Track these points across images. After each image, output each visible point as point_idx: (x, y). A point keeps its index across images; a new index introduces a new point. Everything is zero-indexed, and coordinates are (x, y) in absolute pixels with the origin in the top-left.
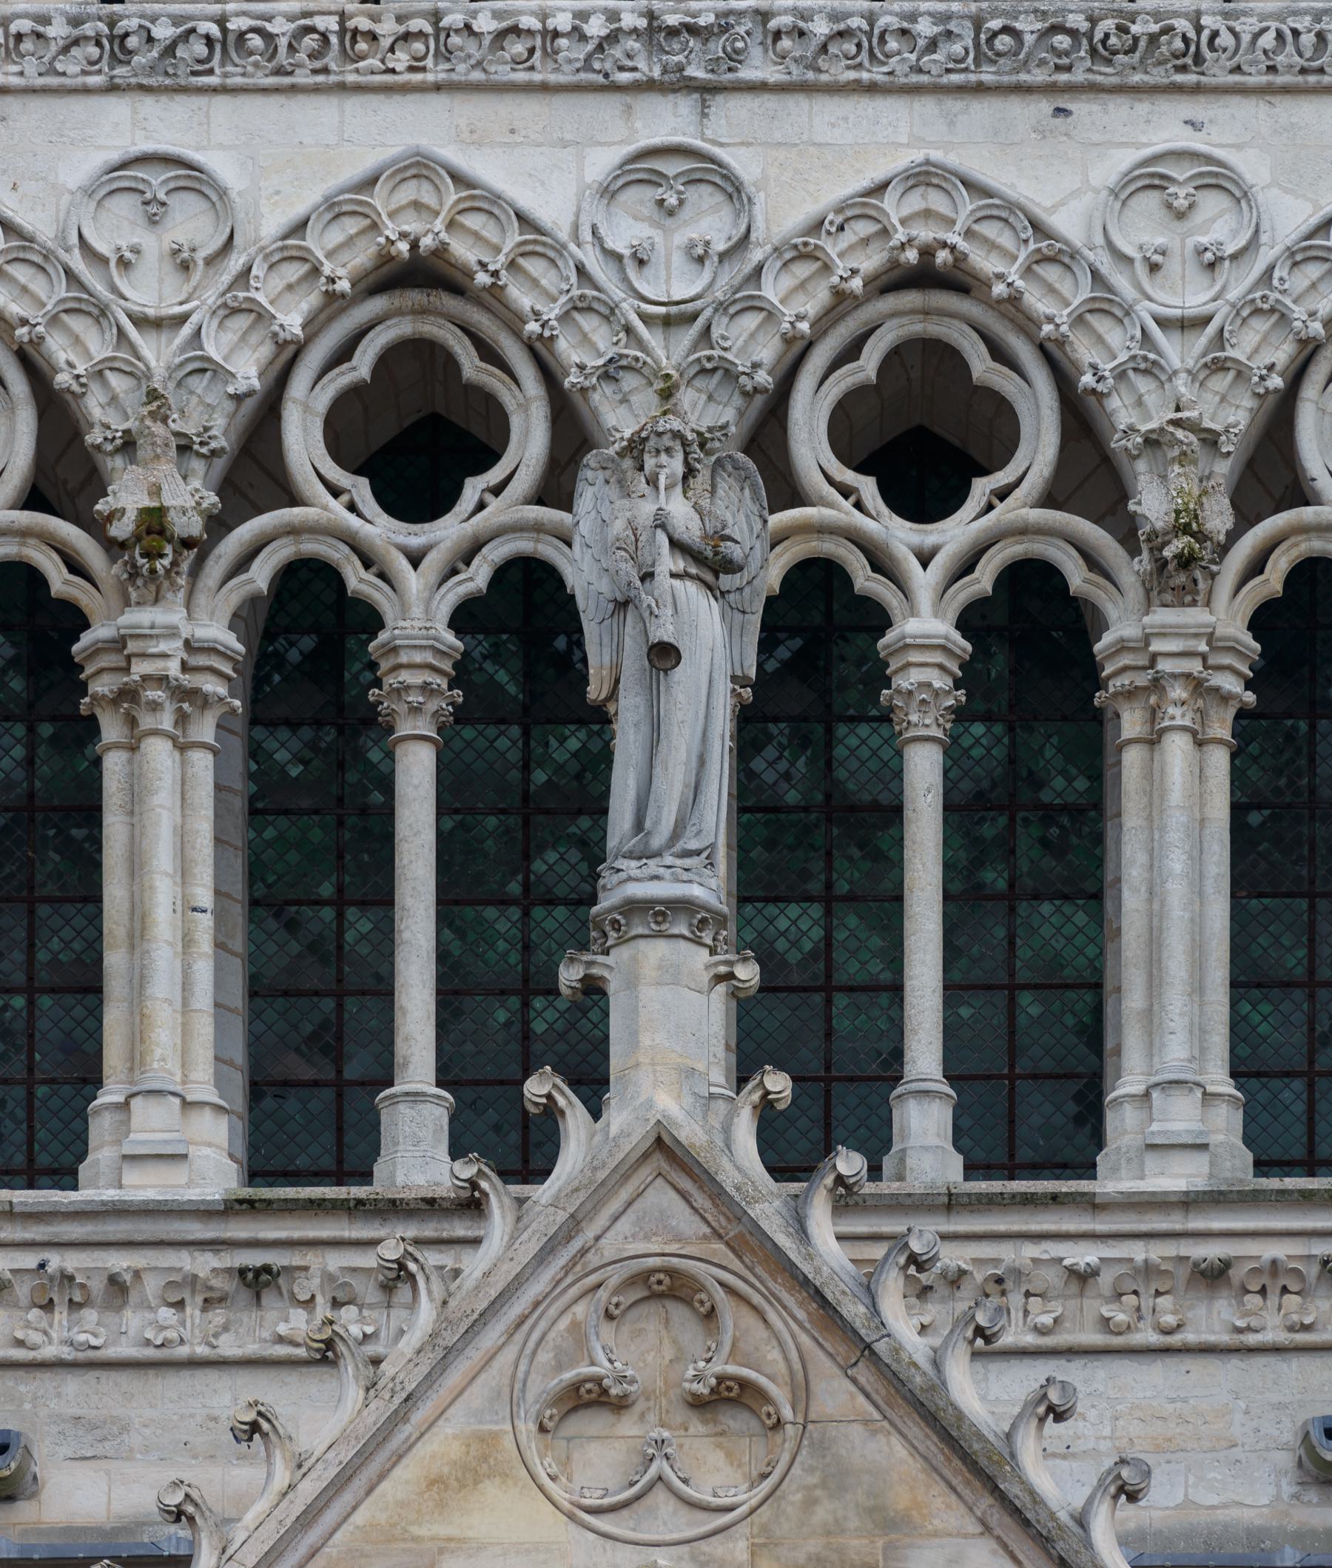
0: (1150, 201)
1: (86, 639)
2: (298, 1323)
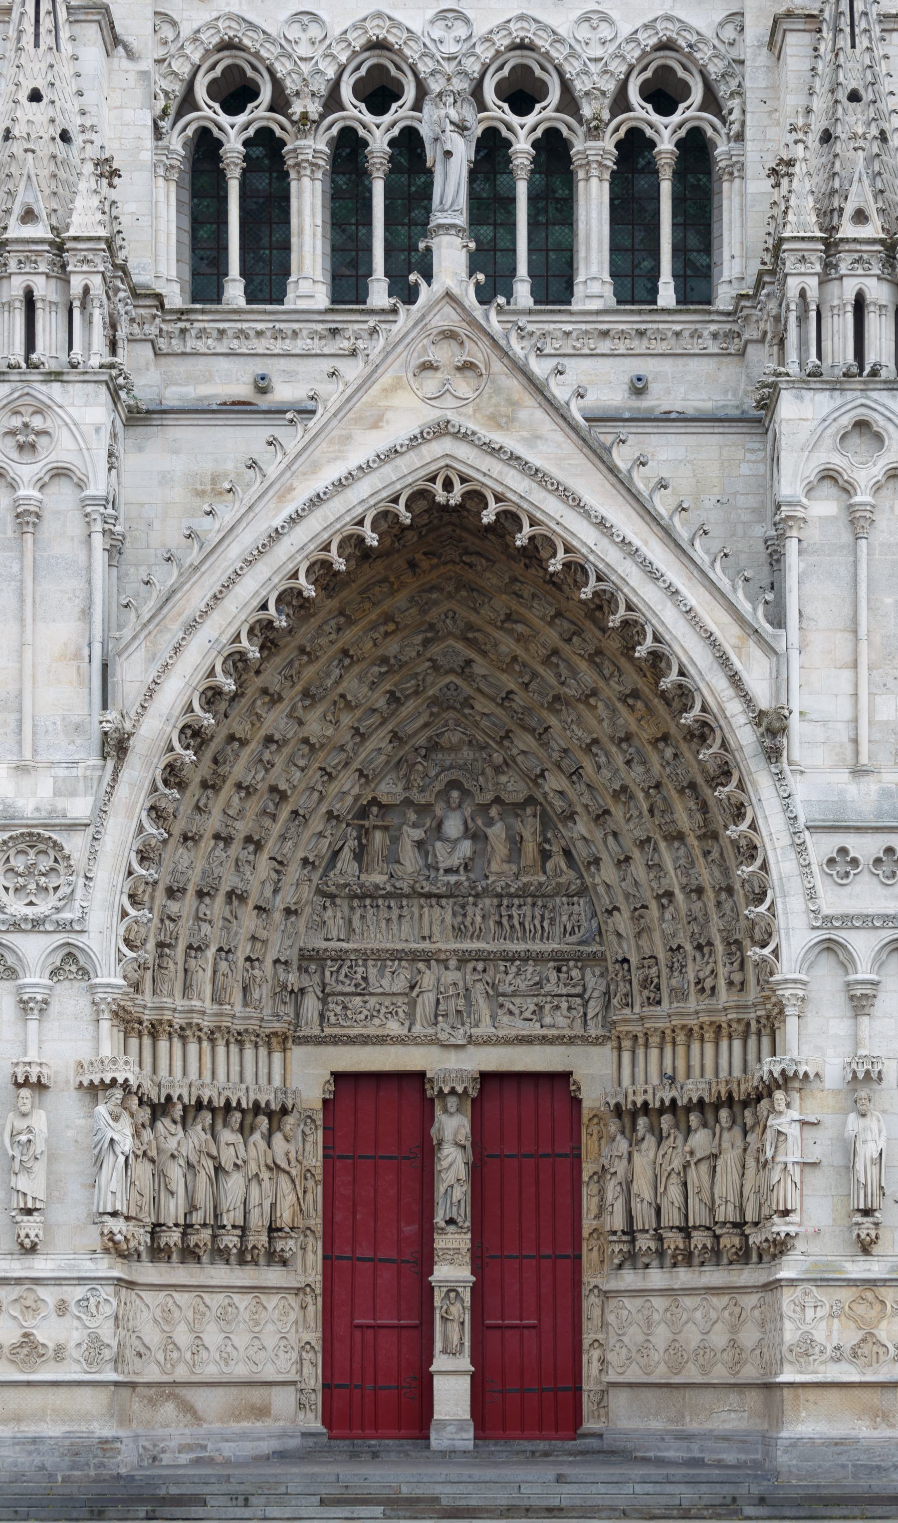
0: (586, 24)
1: (286, 149)
2: (346, 344)
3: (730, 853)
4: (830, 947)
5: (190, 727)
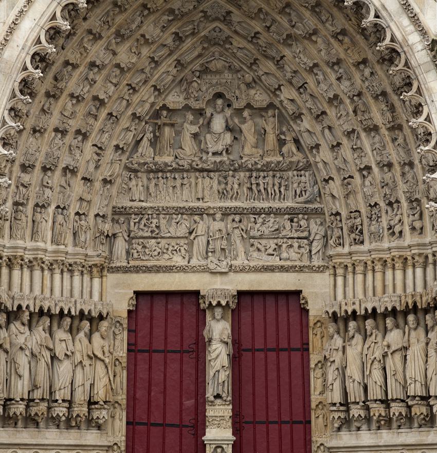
3: (411, 139)
5: (38, 54)
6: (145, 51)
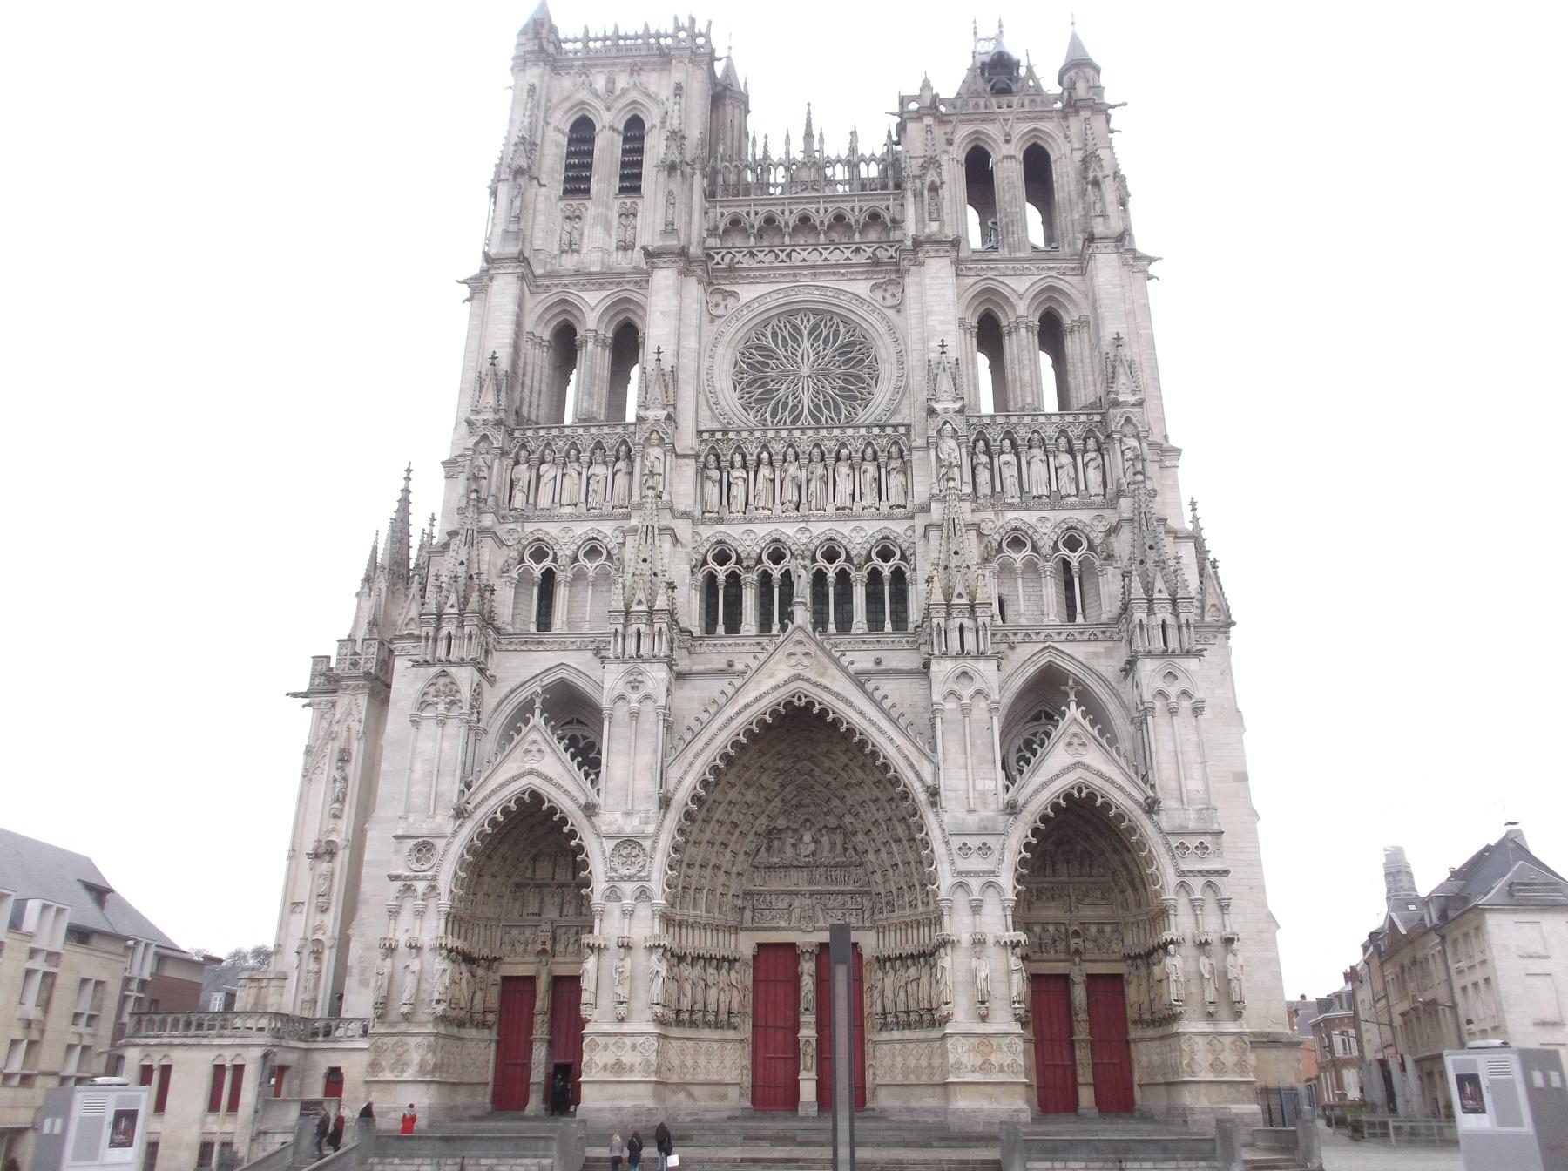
4: (961, 885)
6: (763, 794)
